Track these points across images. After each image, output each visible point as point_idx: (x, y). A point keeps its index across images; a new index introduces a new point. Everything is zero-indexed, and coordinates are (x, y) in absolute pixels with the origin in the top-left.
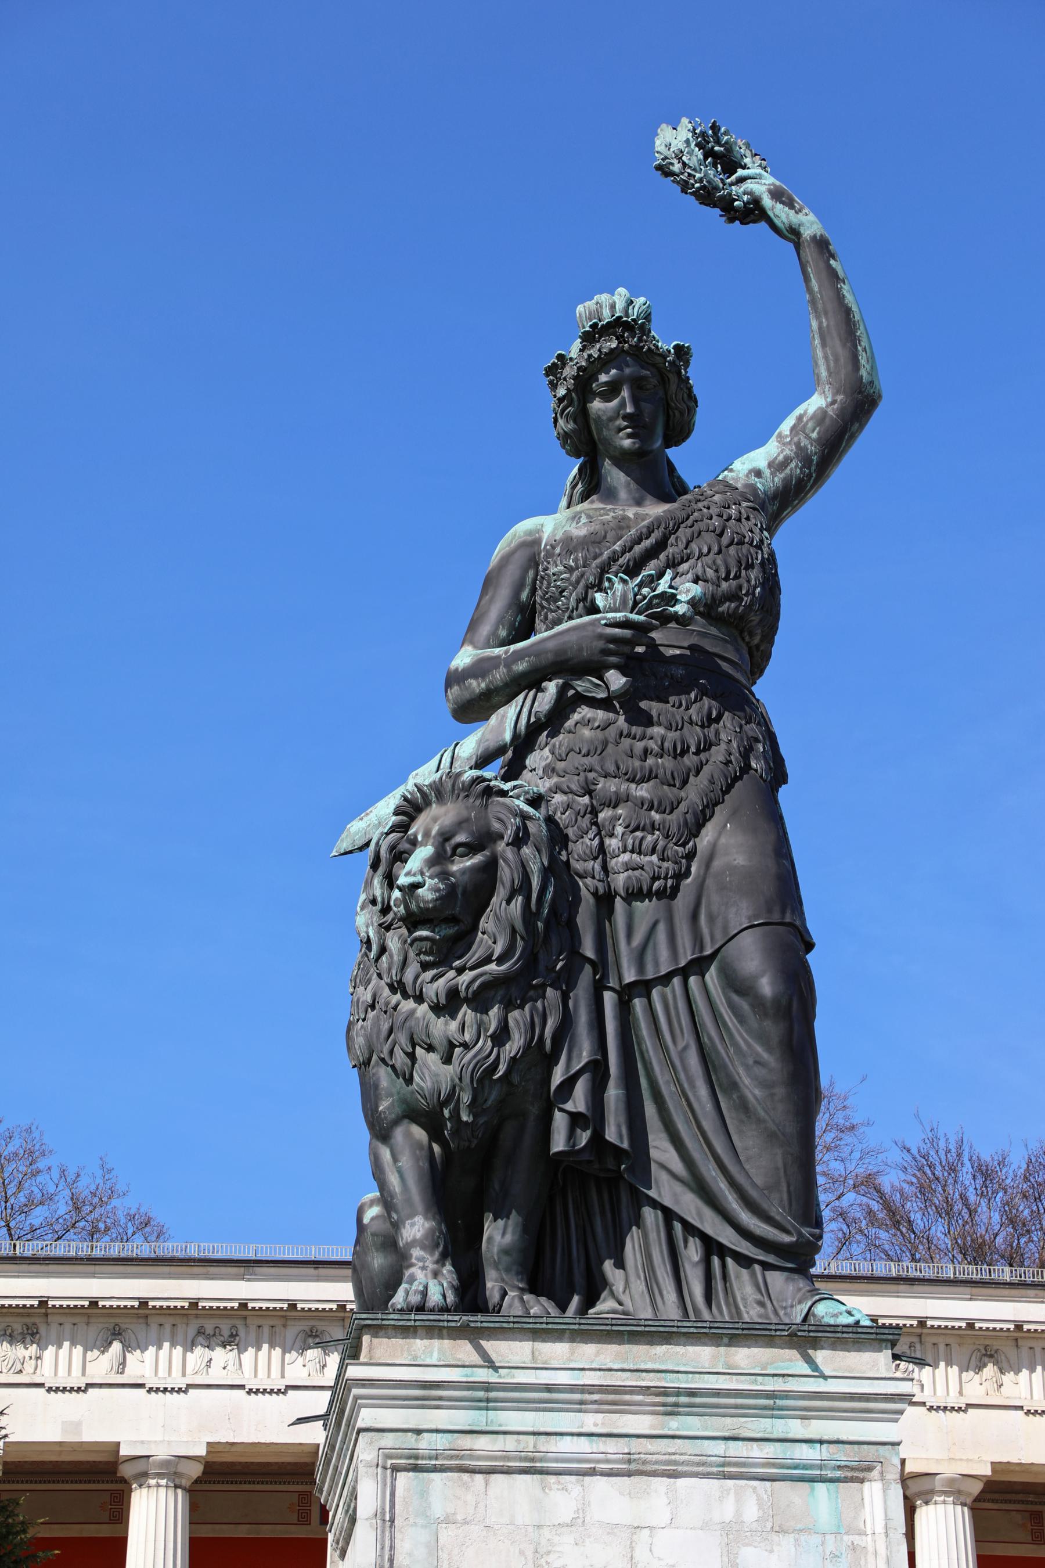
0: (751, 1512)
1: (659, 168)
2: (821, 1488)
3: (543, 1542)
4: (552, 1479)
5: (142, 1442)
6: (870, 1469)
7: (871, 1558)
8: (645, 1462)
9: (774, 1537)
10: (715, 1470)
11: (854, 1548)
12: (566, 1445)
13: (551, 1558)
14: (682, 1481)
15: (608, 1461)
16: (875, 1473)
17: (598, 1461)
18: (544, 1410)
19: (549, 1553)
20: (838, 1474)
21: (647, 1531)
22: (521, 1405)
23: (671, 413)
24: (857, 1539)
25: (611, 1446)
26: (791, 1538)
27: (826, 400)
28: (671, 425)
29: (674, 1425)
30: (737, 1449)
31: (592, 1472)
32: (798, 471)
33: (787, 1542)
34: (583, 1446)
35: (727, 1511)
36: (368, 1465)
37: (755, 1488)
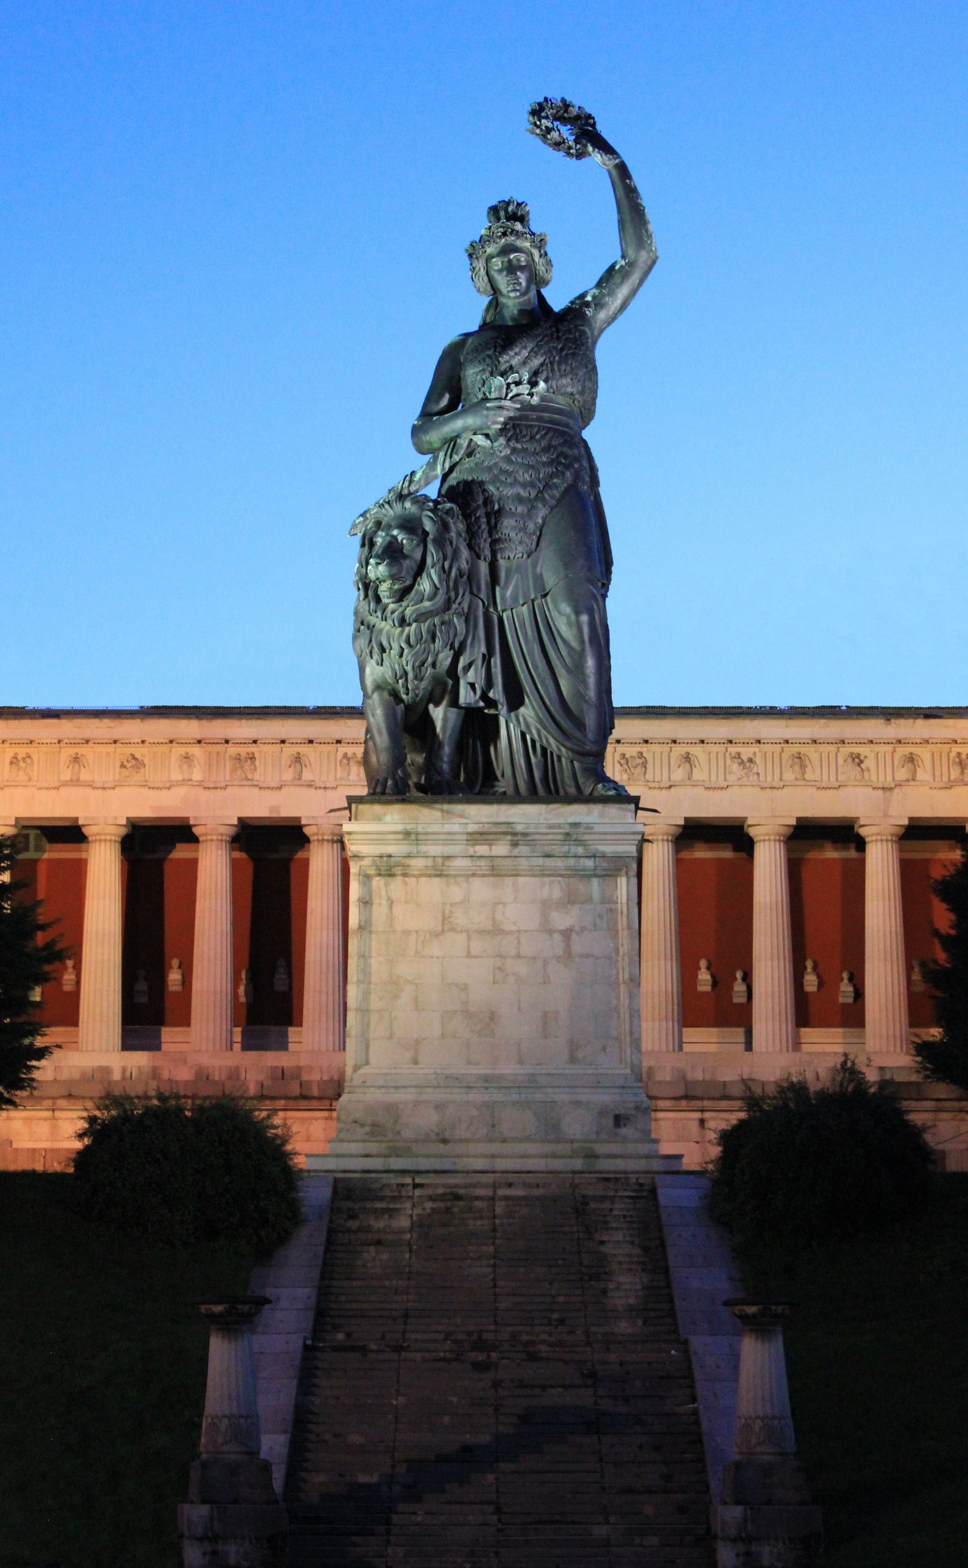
0: (557, 893)
1: (529, 130)
2: (595, 882)
3: (447, 912)
4: (452, 880)
5: (313, 817)
6: (620, 870)
7: (619, 916)
8: (501, 870)
9: (569, 907)
10: (538, 873)
11: (611, 910)
12: (458, 863)
13: (451, 920)
14: (521, 879)
15: (481, 870)
16: (623, 872)
17: (476, 870)
18: (448, 845)
19: (450, 917)
20: (604, 873)
21: (501, 906)
22: (435, 842)
24: (613, 906)
25: (483, 863)
26: (577, 906)
29: (516, 851)
30: (550, 862)
31: (474, 875)
33: (575, 911)
34: (466, 863)
35: (546, 893)
36: (354, 874)
37: (559, 882)
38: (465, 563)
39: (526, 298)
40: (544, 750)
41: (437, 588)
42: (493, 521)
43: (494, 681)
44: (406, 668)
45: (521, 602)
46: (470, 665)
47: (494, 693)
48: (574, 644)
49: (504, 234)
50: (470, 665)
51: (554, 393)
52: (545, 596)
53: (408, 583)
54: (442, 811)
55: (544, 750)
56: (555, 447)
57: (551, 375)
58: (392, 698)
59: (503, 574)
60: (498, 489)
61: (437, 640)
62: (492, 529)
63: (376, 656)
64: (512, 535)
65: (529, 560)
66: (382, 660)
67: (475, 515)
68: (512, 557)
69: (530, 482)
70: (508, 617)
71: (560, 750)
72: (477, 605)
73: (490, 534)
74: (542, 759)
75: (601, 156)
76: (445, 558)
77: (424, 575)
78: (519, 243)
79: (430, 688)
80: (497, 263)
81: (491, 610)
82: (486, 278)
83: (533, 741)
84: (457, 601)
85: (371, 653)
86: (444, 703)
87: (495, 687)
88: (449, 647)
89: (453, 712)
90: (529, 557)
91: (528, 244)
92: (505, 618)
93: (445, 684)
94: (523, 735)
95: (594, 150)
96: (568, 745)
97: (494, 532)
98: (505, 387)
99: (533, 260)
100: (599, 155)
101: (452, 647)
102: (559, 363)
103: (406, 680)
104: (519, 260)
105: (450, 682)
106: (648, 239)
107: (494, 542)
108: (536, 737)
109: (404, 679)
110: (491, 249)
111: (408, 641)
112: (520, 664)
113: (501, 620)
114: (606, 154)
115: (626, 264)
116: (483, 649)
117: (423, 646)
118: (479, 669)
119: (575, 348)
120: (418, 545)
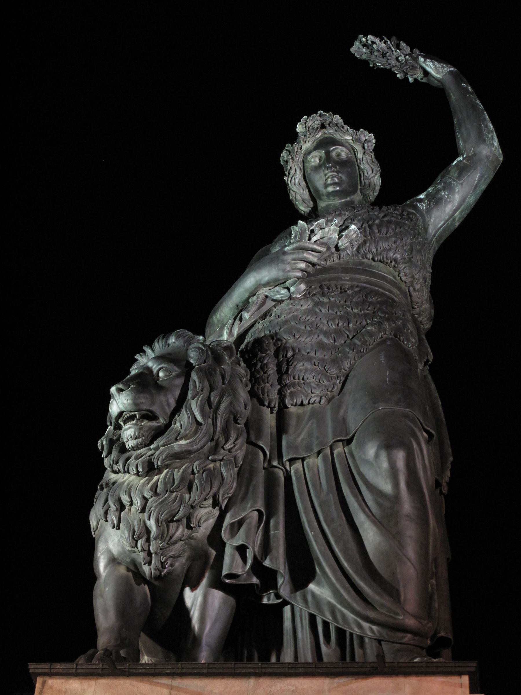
23: (361, 173)
27: (463, 156)
28: (363, 181)
32: (446, 197)
38: (243, 407)
39: (348, 199)
40: (341, 633)
41: (199, 424)
42: (285, 367)
43: (273, 545)
44: (148, 522)
45: (316, 450)
46: (240, 523)
47: (271, 561)
48: (387, 487)
49: (323, 126)
50: (240, 523)
51: (373, 259)
52: (349, 442)
53: (162, 421)
54: (171, 688)
55: (341, 633)
56: (371, 303)
57: (369, 237)
58: (130, 574)
59: (293, 422)
60: (294, 336)
61: (194, 489)
62: (282, 373)
63: (113, 517)
64: (309, 378)
65: (329, 407)
66: (119, 521)
67: (262, 362)
68: (305, 402)
69: (335, 330)
70: (297, 471)
71: (360, 627)
72: (256, 455)
73: (280, 381)
74: (338, 649)
75: (434, 64)
76: (212, 389)
77: (183, 411)
78: (338, 136)
79: (186, 567)
80: (314, 159)
81: (275, 463)
82: (303, 183)
83: (326, 625)
84: (228, 446)
85: (106, 513)
86: (204, 582)
87: (274, 551)
88: (210, 501)
89: (217, 595)
90: (329, 402)
91: (349, 138)
92: (292, 472)
93: (206, 556)
94: (312, 618)
95: (425, 61)
96: (371, 614)
97: (285, 377)
98: (308, 233)
99: (356, 158)
100: (431, 64)
101: (215, 504)
102: (379, 226)
103: (148, 540)
104: (339, 155)
105: (213, 553)
106: (489, 133)
107: (283, 387)
108: (329, 618)
109: (144, 538)
110: (307, 145)
111: (154, 490)
112: (309, 522)
113: (288, 478)
114: (439, 62)
115: (464, 159)
116: (260, 505)
117: (174, 494)
118: (253, 530)
119: (400, 219)
120: (178, 376)
